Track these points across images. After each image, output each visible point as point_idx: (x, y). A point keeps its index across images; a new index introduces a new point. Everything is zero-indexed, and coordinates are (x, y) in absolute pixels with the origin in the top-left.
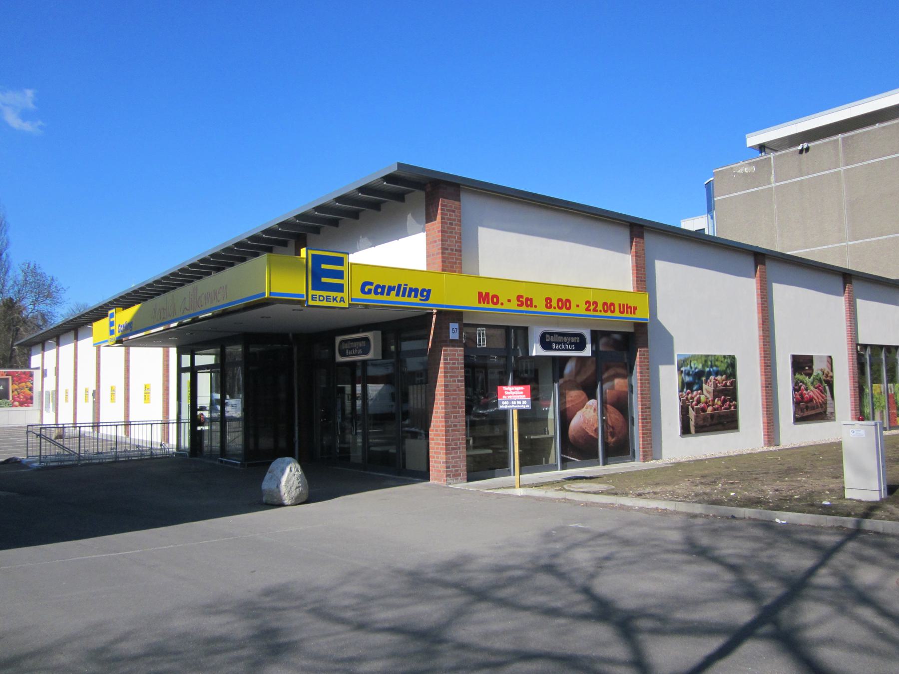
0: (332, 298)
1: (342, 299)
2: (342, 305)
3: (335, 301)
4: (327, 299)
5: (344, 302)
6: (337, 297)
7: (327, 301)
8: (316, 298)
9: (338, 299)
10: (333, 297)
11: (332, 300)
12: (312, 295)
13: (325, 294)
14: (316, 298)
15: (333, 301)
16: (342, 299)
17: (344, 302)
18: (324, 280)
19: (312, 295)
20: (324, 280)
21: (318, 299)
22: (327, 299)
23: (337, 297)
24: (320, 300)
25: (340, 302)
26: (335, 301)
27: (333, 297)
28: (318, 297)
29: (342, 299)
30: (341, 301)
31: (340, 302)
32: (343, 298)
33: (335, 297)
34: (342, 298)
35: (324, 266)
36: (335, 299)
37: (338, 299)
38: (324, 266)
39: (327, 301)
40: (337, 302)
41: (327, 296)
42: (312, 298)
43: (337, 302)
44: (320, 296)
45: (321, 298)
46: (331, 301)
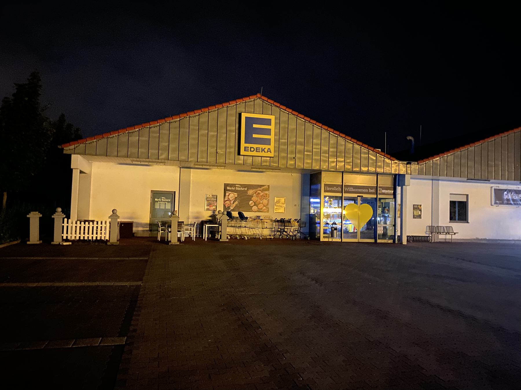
0: (261, 149)
1: (269, 150)
2: (269, 154)
3: (263, 152)
4: (257, 150)
5: (271, 152)
7: (256, 151)
9: (266, 150)
10: (262, 148)
11: (261, 152)
12: (245, 147)
13: (255, 146)
14: (248, 149)
15: (262, 152)
16: (269, 150)
17: (271, 152)
18: (254, 136)
19: (245, 147)
20: (254, 136)
21: (249, 150)
22: (257, 150)
24: (251, 151)
25: (267, 152)
26: (263, 152)
27: (262, 148)
28: (249, 148)
29: (269, 150)
31: (267, 152)
33: (263, 149)
36: (263, 150)
37: (266, 150)
39: (256, 151)
40: (265, 152)
41: (257, 148)
42: (245, 149)
43: (265, 152)
44: (251, 148)
45: (252, 149)
46: (260, 152)
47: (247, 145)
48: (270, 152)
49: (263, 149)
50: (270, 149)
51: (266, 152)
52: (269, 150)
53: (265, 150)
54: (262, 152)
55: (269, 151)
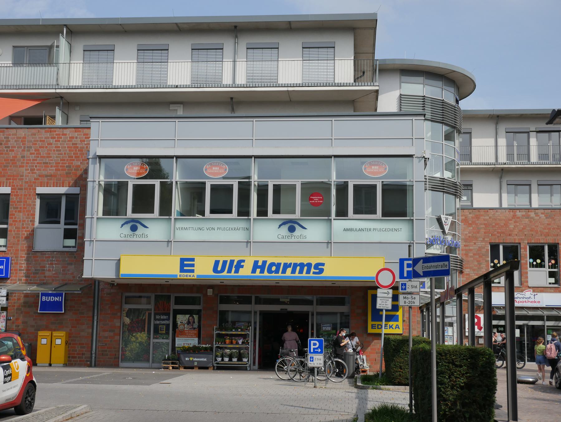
1: (397, 327)
3: (391, 328)
5: (399, 329)
6: (392, 325)
8: (376, 327)
9: (394, 327)
10: (390, 325)
11: (388, 329)
12: (372, 325)
14: (376, 327)
15: (390, 328)
16: (397, 327)
17: (399, 329)
19: (372, 325)
21: (377, 327)
23: (392, 325)
24: (378, 328)
25: (395, 329)
26: (391, 328)
27: (390, 325)
28: (377, 326)
29: (397, 327)
30: (396, 328)
31: (395, 329)
32: (398, 326)
33: (391, 325)
34: (397, 325)
35: (185, 263)
37: (394, 327)
38: (185, 263)
40: (393, 328)
43: (393, 328)
44: (378, 325)
47: (374, 323)
48: (398, 329)
49: (391, 325)
50: (398, 325)
51: (394, 328)
52: (397, 327)
53: (393, 326)
54: (390, 328)
55: (397, 328)
